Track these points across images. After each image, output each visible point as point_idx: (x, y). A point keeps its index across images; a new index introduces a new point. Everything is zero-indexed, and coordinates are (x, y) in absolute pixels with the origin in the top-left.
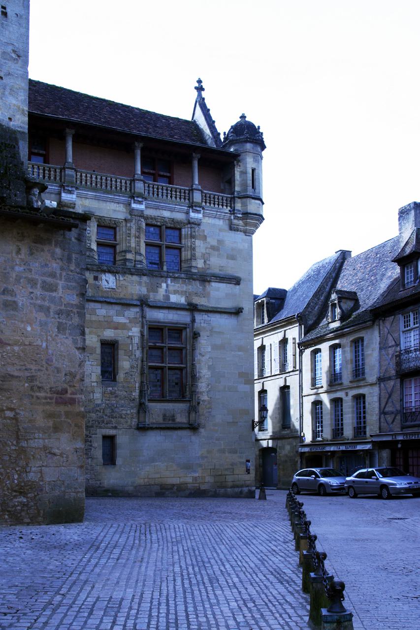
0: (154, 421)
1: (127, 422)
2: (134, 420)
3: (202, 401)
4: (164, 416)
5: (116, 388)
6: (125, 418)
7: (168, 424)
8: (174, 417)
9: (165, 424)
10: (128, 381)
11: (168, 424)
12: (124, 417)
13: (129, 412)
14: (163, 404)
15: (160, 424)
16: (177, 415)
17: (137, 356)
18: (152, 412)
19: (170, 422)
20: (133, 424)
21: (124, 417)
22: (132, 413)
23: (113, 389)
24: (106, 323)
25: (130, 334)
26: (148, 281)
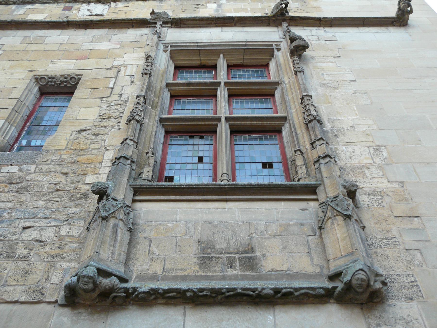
0: (157, 269)
1: (26, 273)
2: (66, 265)
3: (372, 193)
4: (204, 250)
5: (32, 168)
6: (25, 258)
7: (224, 278)
8: (252, 250)
9: (207, 278)
10: (82, 146)
11: (224, 278)
12: (25, 252)
13: (49, 234)
14: (200, 205)
15: (184, 278)
16: (267, 243)
17: (124, 97)
18: (153, 234)
19: (230, 272)
20: (55, 280)
21: (25, 252)
22: (61, 238)
23: (20, 170)
24: (61, 52)
25: (116, 63)
26: (176, 4)
